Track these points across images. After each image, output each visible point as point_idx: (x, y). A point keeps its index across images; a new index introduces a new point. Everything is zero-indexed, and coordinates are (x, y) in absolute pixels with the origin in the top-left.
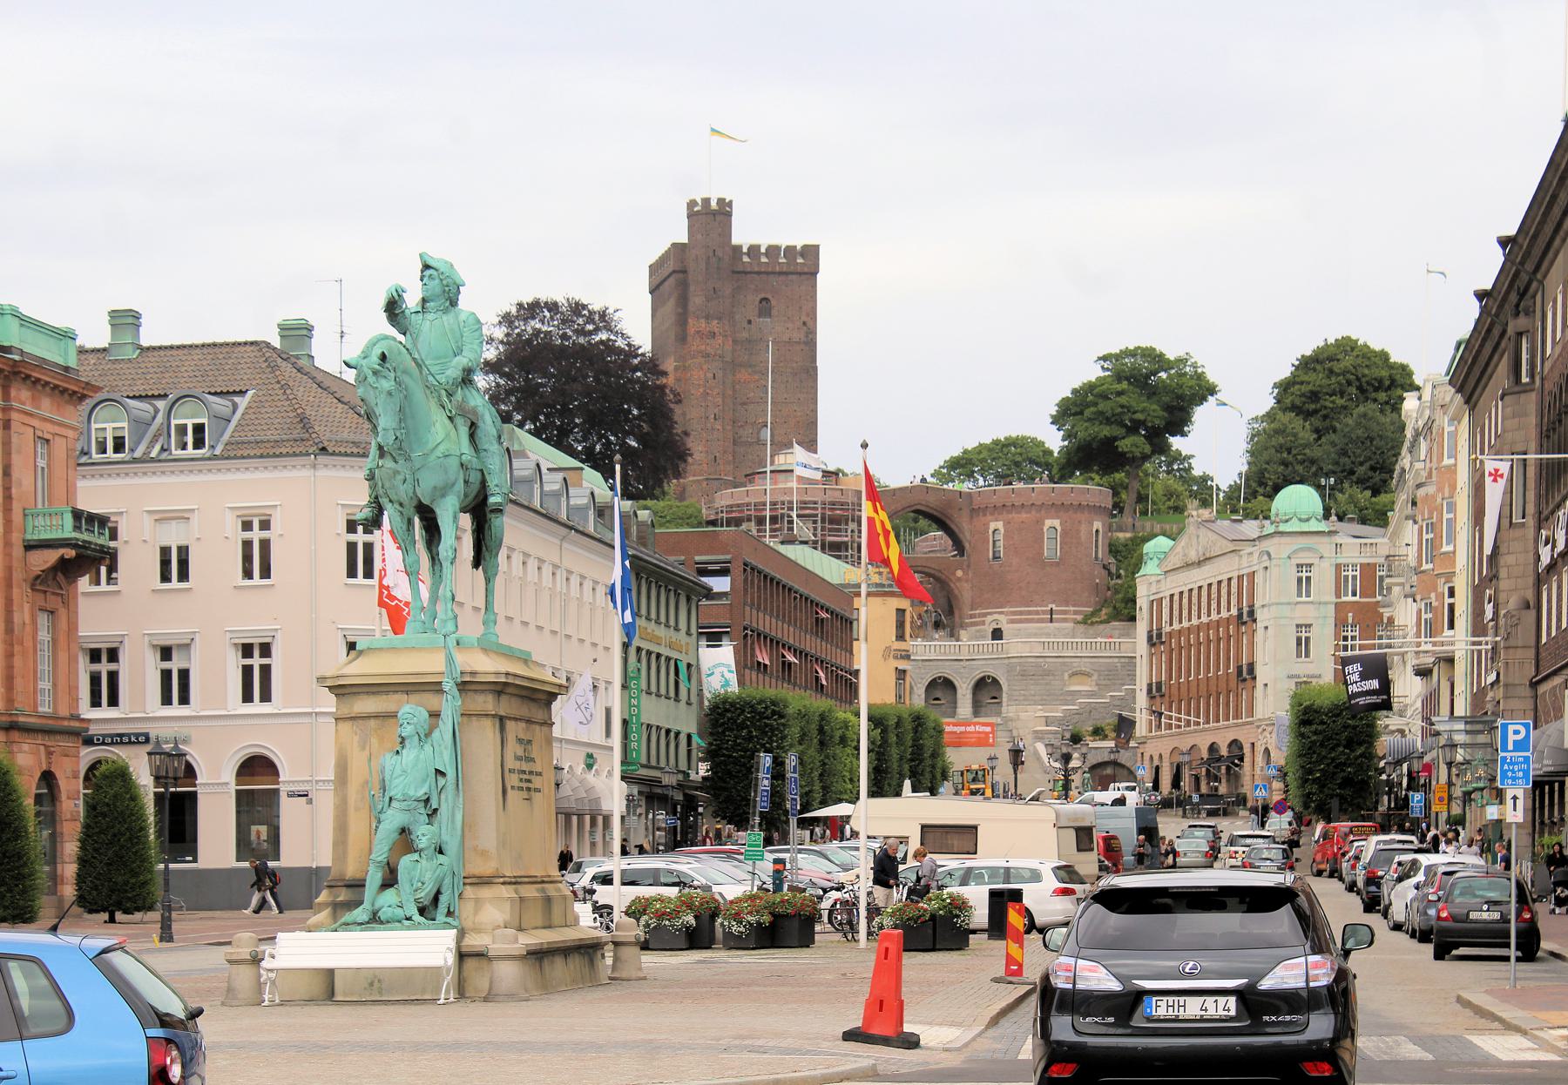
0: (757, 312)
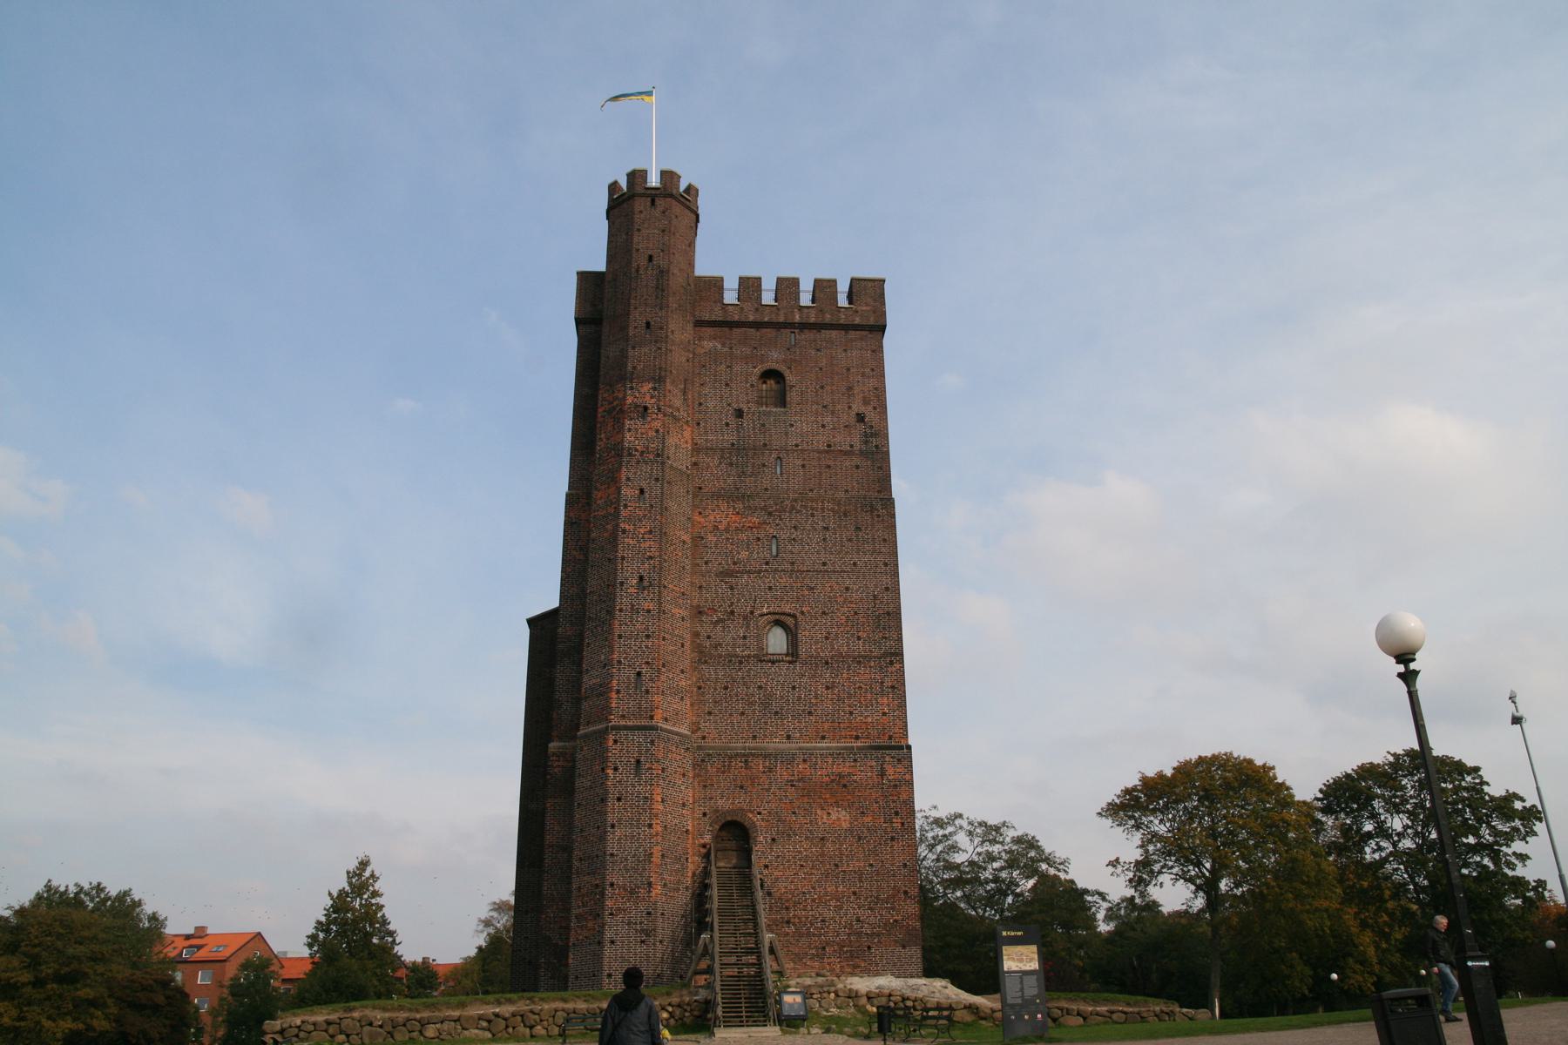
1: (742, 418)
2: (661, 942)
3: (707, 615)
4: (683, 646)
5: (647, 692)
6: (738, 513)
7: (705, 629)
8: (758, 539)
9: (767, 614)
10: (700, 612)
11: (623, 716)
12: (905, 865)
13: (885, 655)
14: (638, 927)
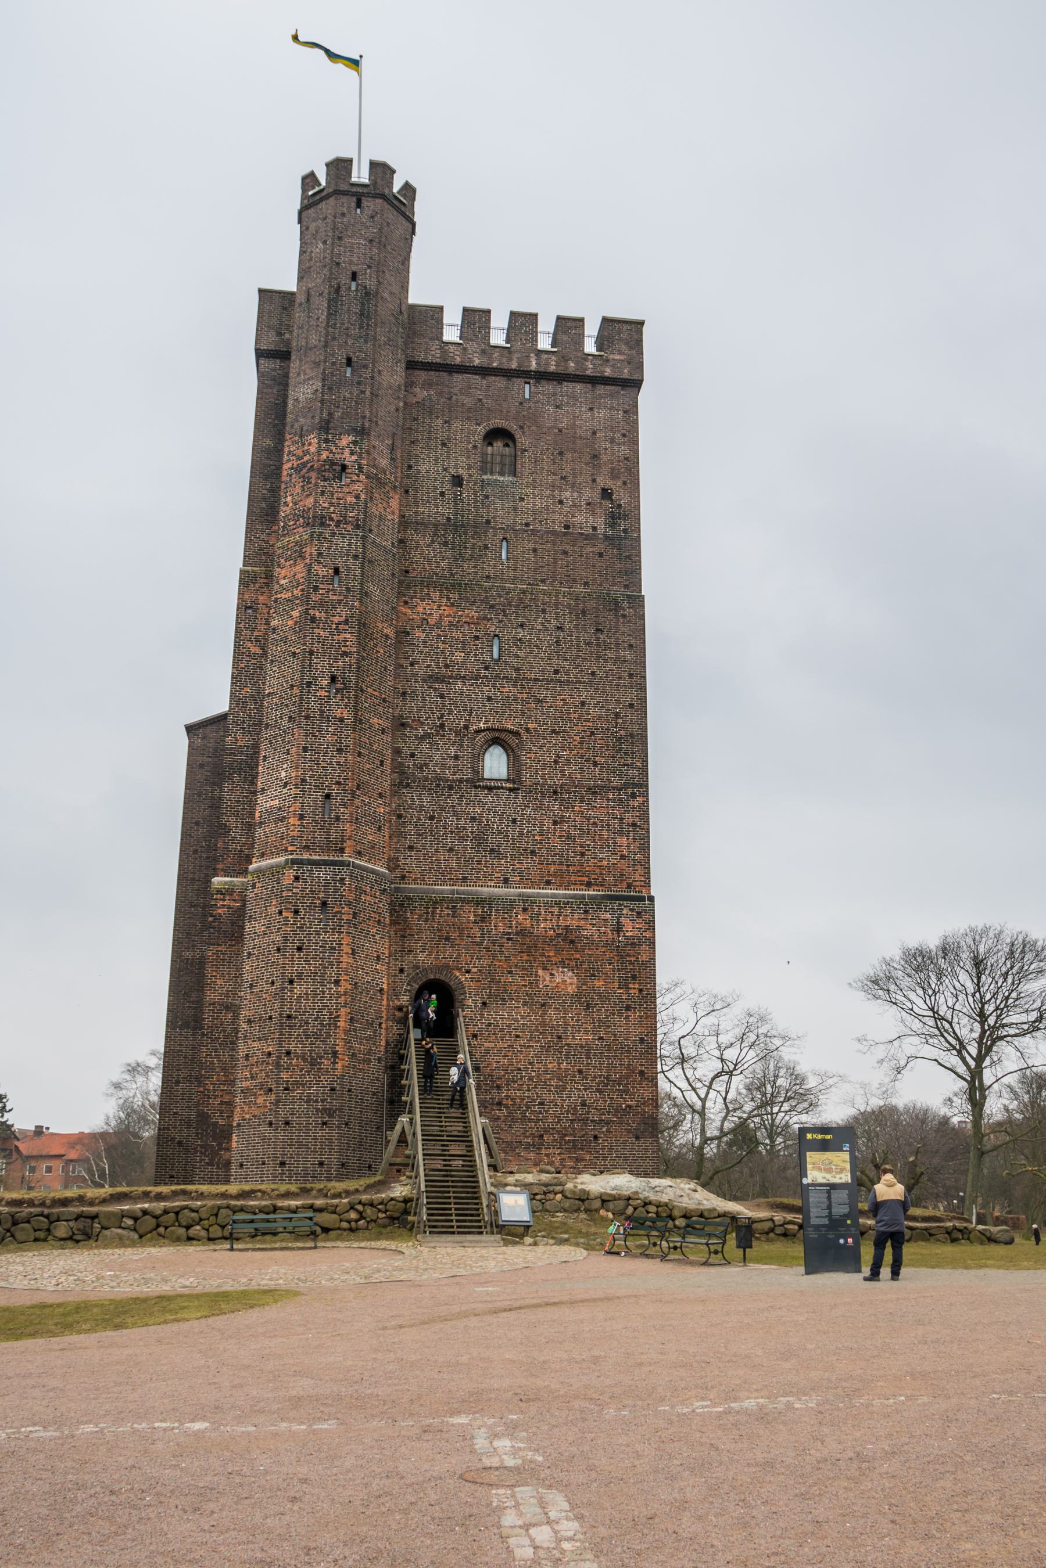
0: (475, 459)
1: (461, 487)
2: (346, 1124)
3: (412, 728)
4: (382, 763)
5: (338, 818)
6: (453, 605)
7: (408, 746)
8: (477, 638)
9: (484, 731)
10: (403, 725)
11: (307, 847)
12: (642, 1040)
13: (626, 785)
14: (320, 1106)
